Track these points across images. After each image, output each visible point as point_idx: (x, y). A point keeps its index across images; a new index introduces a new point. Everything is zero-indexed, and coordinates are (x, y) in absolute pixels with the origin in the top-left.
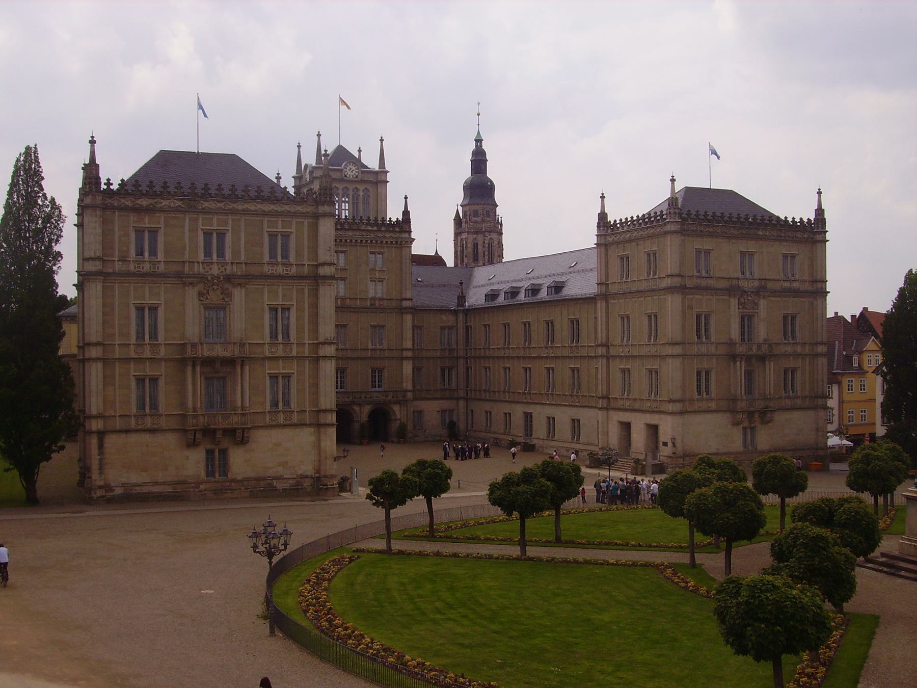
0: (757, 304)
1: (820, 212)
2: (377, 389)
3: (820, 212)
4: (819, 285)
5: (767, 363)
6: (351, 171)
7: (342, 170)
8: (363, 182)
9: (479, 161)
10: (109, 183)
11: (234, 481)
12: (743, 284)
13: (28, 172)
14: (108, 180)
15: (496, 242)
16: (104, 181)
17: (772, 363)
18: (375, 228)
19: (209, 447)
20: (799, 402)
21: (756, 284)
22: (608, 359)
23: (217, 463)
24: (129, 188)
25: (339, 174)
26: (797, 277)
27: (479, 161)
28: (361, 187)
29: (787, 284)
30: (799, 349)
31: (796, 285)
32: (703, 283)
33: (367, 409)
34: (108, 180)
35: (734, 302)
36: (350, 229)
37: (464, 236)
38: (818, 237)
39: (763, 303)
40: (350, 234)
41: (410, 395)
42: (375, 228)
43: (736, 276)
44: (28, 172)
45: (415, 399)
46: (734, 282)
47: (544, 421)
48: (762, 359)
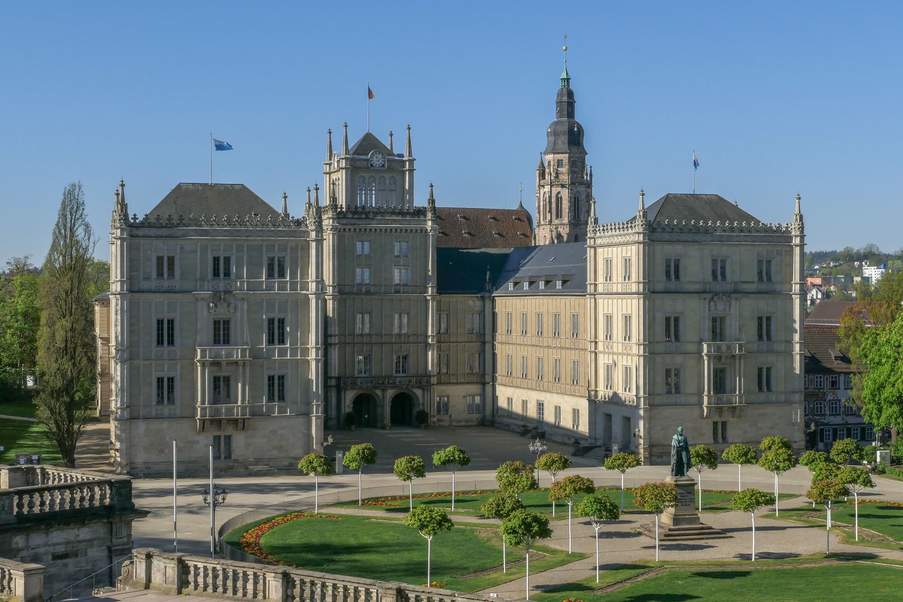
2: (401, 374)
6: (377, 160)
7: (368, 160)
9: (568, 103)
10: (135, 218)
11: (236, 461)
13: (72, 208)
14: (135, 215)
15: (584, 196)
16: (131, 216)
19: (217, 433)
22: (596, 354)
23: (223, 447)
24: (152, 220)
25: (365, 163)
27: (568, 103)
33: (390, 393)
34: (135, 215)
37: (547, 189)
41: (434, 380)
44: (72, 208)
45: (440, 383)
47: (553, 410)
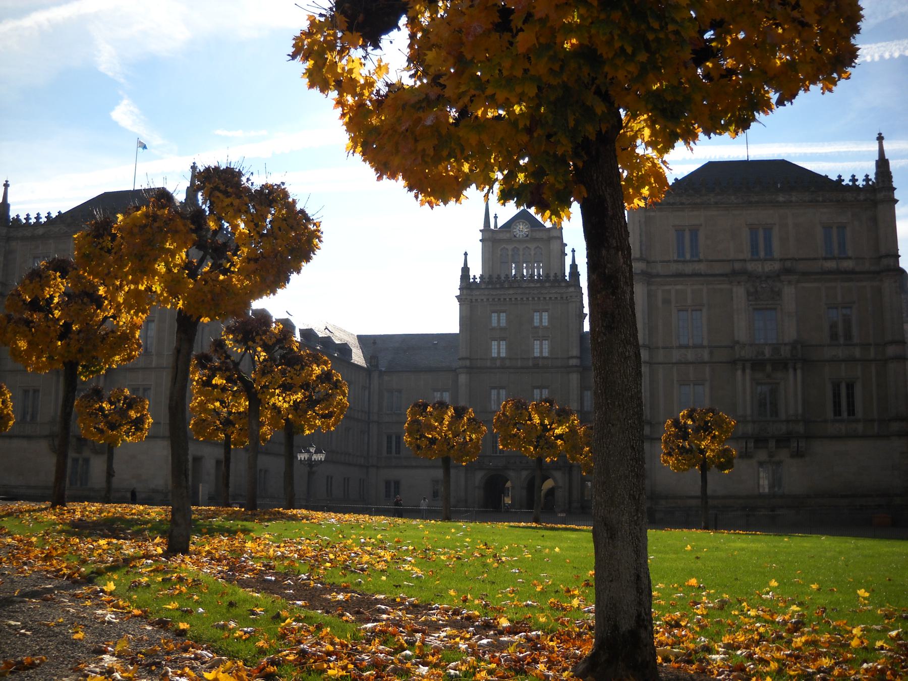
0: (779, 294)
1: (883, 164)
3: (883, 164)
4: (885, 262)
5: (791, 371)
8: (534, 240)
12: (750, 267)
17: (799, 372)
18: (538, 285)
20: (860, 427)
21: (777, 266)
26: (850, 253)
28: (532, 246)
29: (831, 265)
30: (857, 353)
31: (848, 265)
32: (688, 269)
35: (740, 291)
36: (510, 287)
38: (880, 196)
39: (789, 292)
40: (511, 292)
42: (538, 285)
43: (741, 257)
46: (737, 266)
48: (781, 365)
